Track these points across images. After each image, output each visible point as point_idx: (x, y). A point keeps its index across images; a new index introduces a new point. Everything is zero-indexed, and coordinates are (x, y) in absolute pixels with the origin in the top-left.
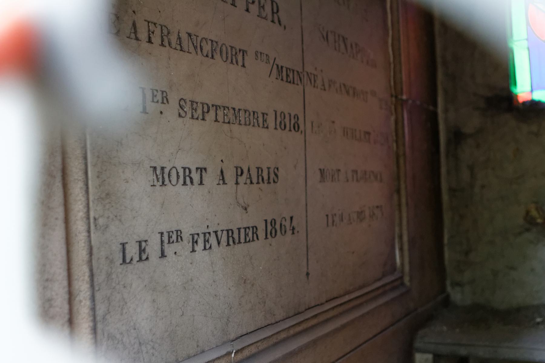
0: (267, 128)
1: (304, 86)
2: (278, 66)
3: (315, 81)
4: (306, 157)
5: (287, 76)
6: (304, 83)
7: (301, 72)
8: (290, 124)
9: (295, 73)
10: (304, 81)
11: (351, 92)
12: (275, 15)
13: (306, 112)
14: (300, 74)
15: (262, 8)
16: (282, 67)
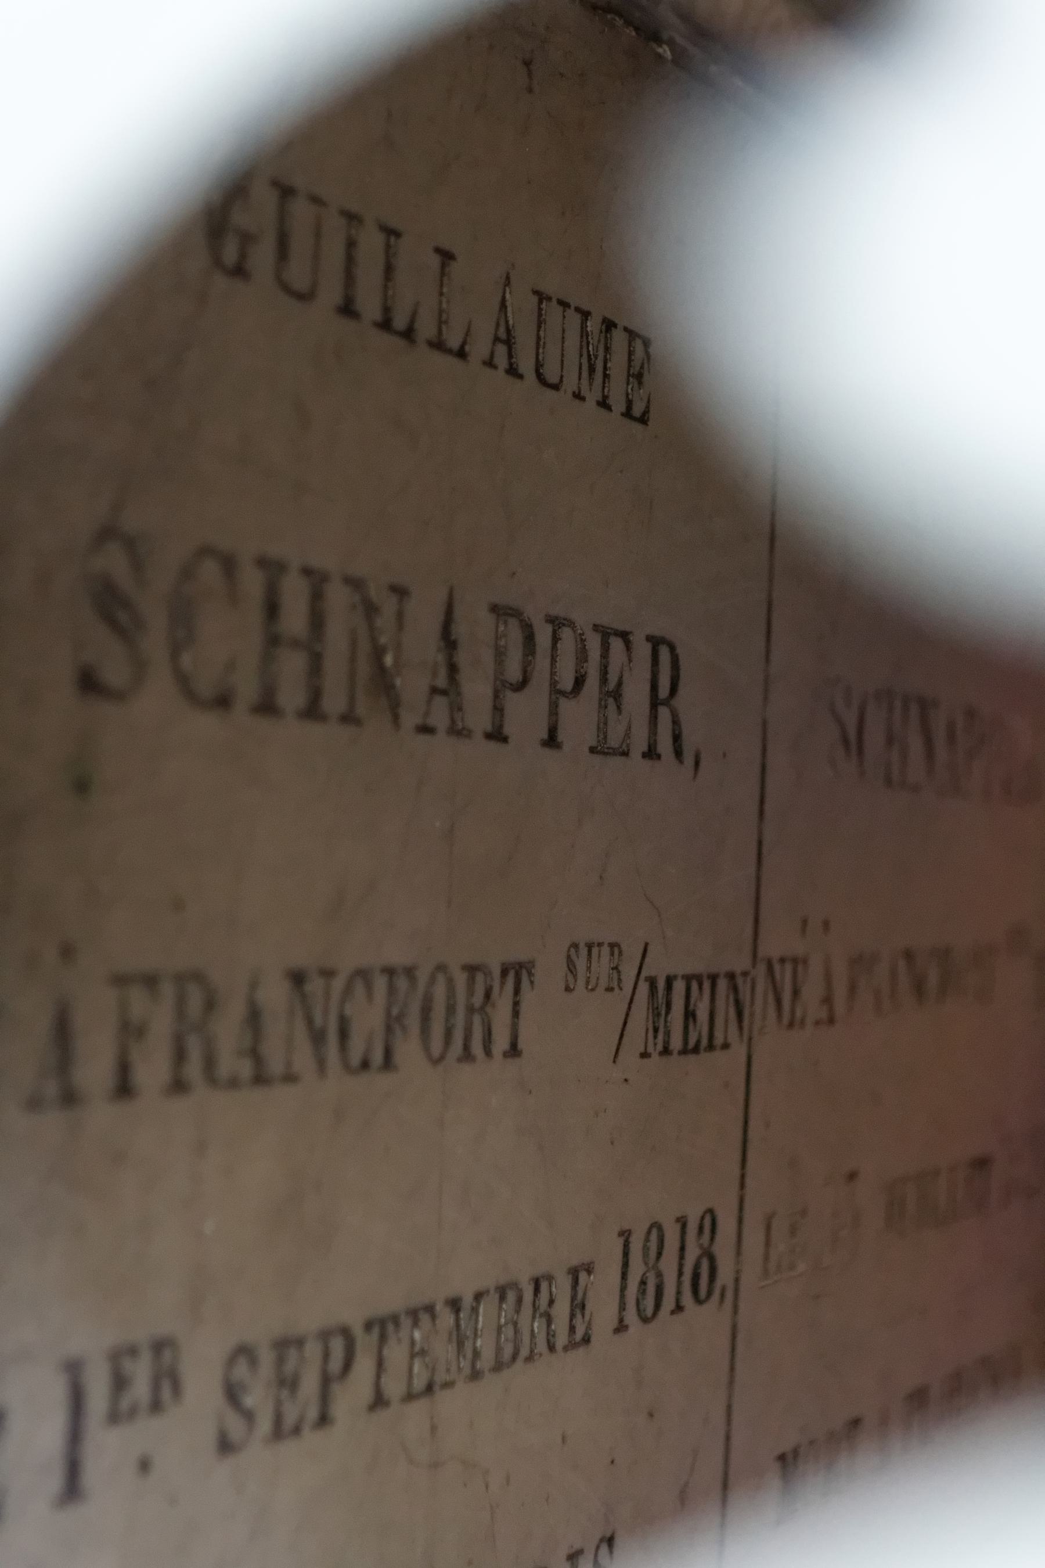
0: (586, 1340)
1: (750, 1039)
2: (652, 982)
3: (796, 993)
4: (729, 1421)
5: (690, 1015)
6: (751, 1031)
7: (745, 974)
8: (680, 1273)
9: (722, 984)
10: (752, 1014)
11: (933, 978)
12: (664, 712)
13: (748, 1181)
14: (740, 981)
15: (611, 700)
16: (669, 981)
